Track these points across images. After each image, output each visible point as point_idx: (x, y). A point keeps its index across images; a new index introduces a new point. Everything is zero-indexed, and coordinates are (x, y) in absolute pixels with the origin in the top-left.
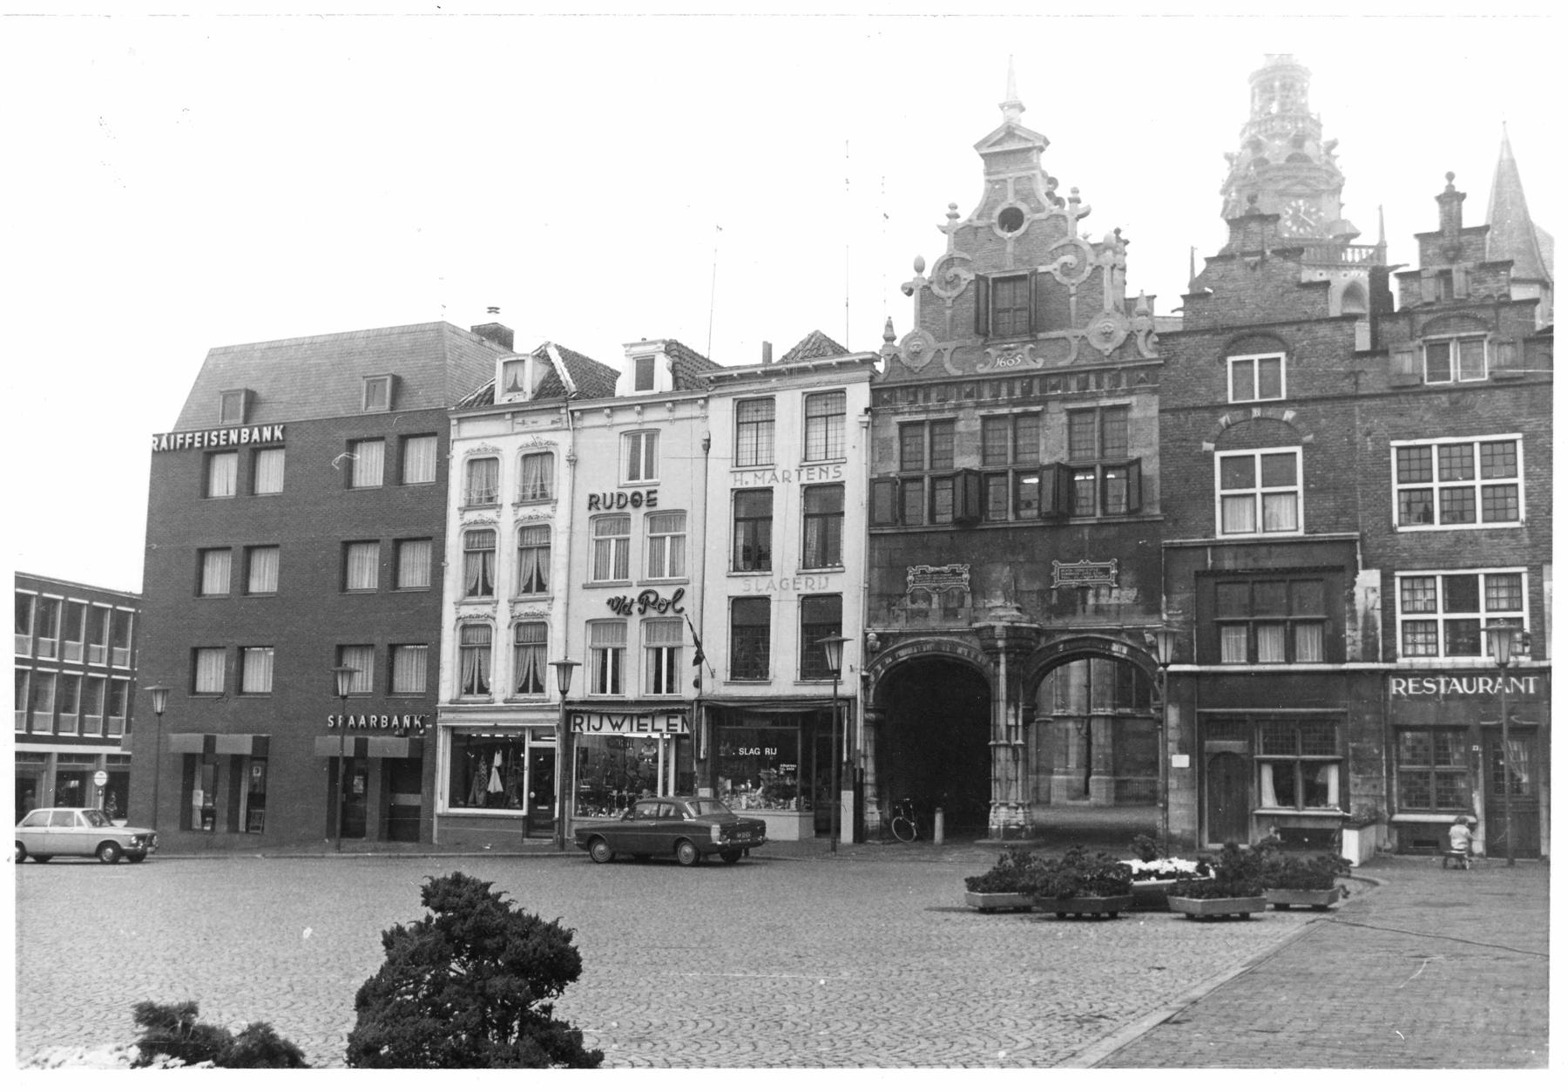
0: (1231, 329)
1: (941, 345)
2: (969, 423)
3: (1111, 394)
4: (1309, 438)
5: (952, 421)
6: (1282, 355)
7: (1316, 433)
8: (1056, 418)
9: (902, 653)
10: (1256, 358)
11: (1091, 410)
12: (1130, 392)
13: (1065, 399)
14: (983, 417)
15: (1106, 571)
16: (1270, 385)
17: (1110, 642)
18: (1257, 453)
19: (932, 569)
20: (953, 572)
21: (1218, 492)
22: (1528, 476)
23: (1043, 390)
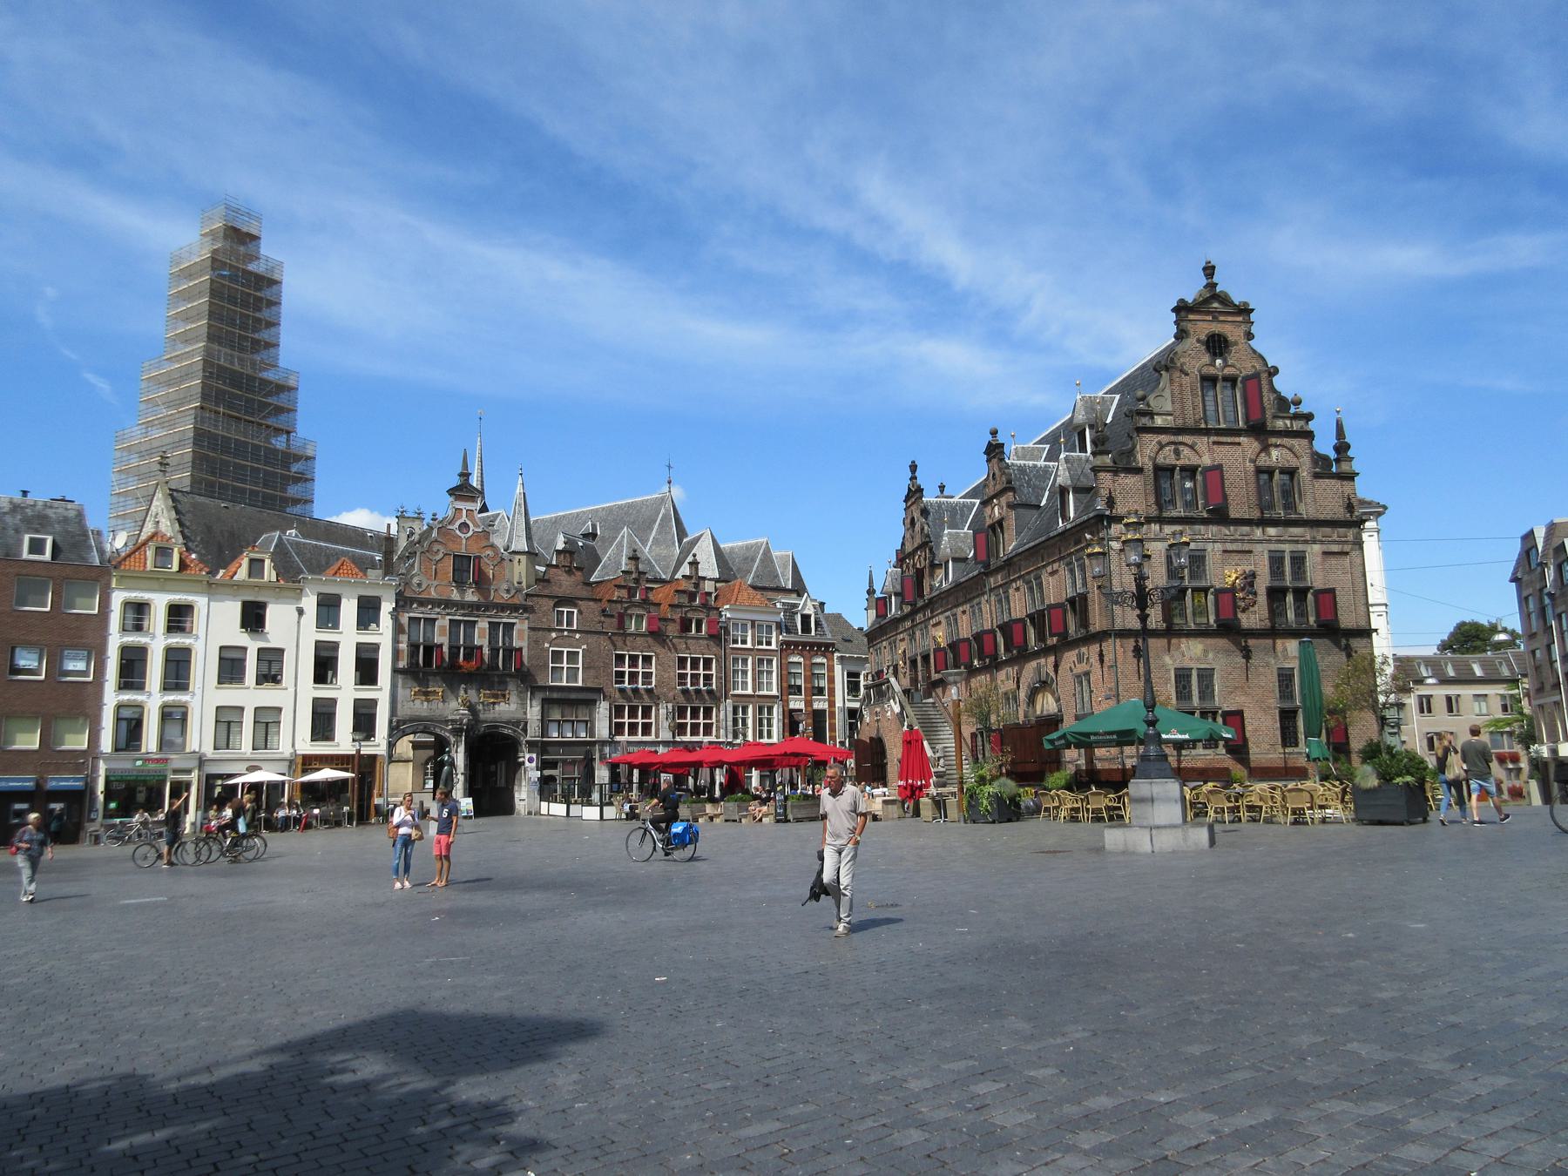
2: (443, 622)
8: (483, 624)
16: (570, 623)
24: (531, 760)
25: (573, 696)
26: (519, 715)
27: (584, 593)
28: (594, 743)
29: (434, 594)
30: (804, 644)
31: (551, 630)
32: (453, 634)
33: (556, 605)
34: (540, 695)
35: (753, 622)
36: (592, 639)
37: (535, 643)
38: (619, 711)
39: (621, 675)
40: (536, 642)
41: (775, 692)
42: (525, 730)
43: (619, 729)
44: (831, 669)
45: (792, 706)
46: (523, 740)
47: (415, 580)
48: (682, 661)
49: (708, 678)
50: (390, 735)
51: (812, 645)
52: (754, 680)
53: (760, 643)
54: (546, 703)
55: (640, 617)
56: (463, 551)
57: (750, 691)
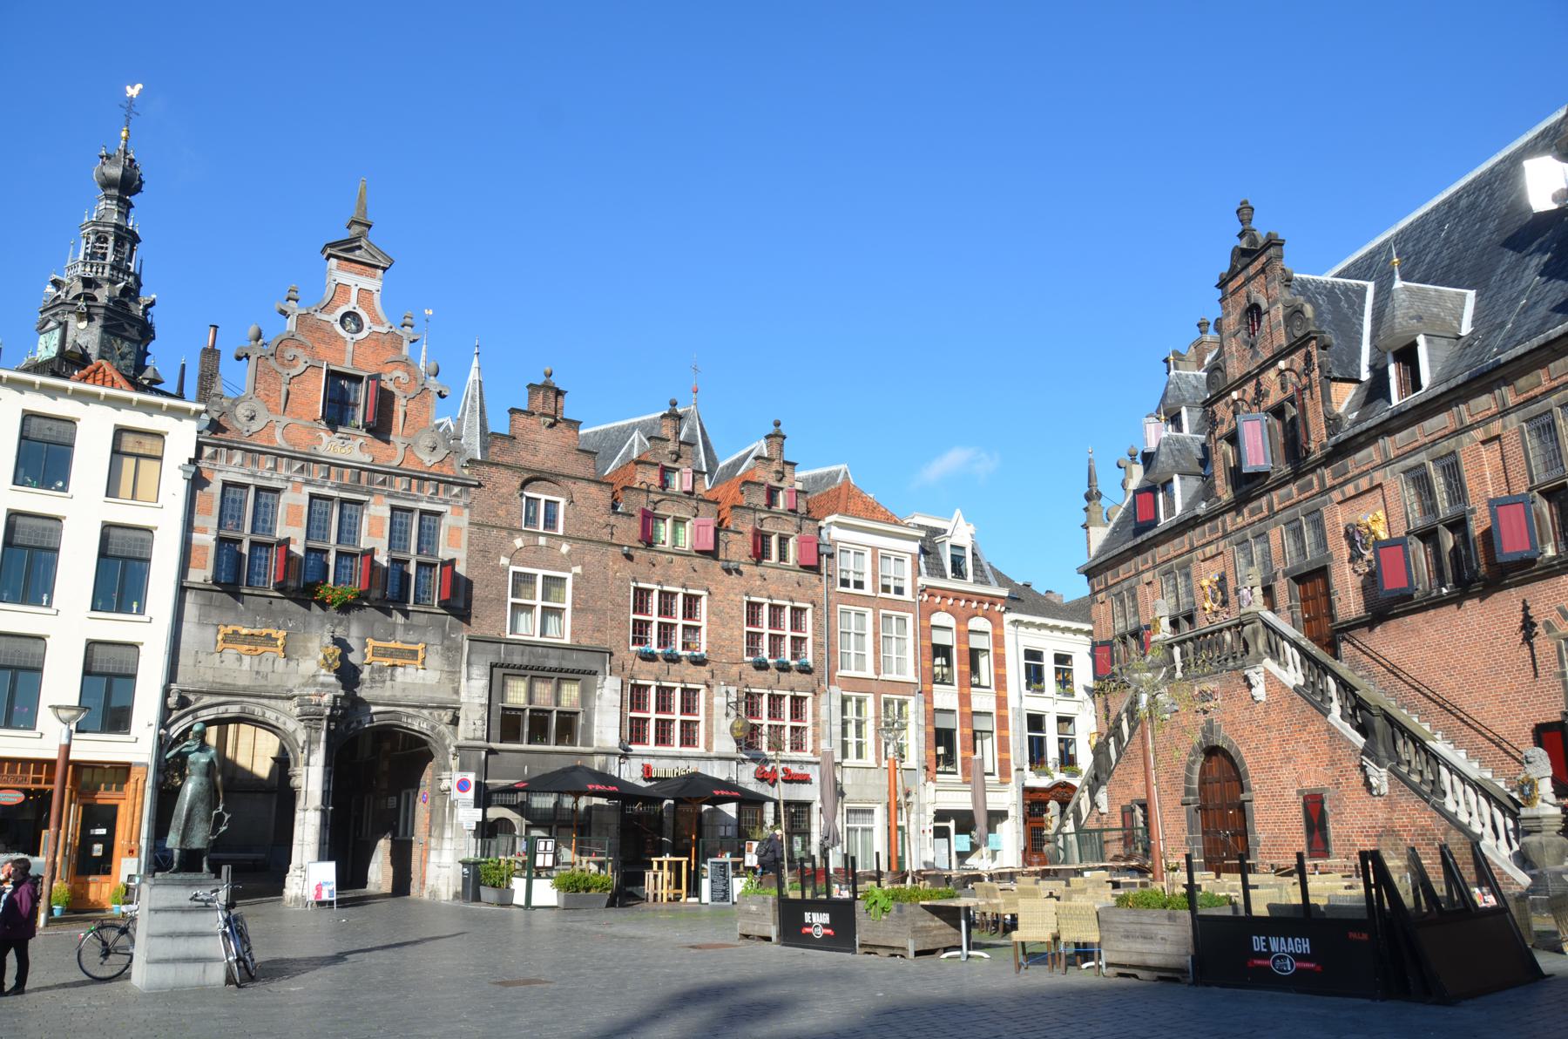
0: (529, 470)
1: (274, 418)
3: (431, 500)
4: (578, 569)
5: (277, 491)
6: (562, 502)
7: (583, 566)
9: (204, 712)
10: (543, 497)
11: (411, 510)
12: (446, 502)
13: (390, 495)
14: (312, 497)
15: (414, 654)
16: (550, 521)
17: (408, 716)
18: (540, 573)
19: (245, 631)
20: (269, 635)
21: (511, 600)
22: (708, 621)
23: (370, 482)
24: (463, 785)
25: (553, 663)
26: (444, 695)
27: (580, 471)
28: (592, 754)
29: (279, 441)
30: (958, 595)
31: (513, 531)
32: (315, 525)
33: (524, 485)
34: (490, 655)
35: (875, 549)
36: (592, 555)
37: (482, 552)
38: (637, 695)
39: (641, 628)
40: (484, 552)
41: (910, 676)
42: (455, 721)
43: (636, 731)
44: (999, 641)
45: (937, 704)
46: (451, 743)
47: (242, 411)
48: (754, 608)
49: (797, 642)
50: (164, 723)
51: (969, 597)
52: (876, 652)
53: (886, 588)
54: (500, 673)
55: (679, 522)
56: (346, 367)
57: (869, 673)
